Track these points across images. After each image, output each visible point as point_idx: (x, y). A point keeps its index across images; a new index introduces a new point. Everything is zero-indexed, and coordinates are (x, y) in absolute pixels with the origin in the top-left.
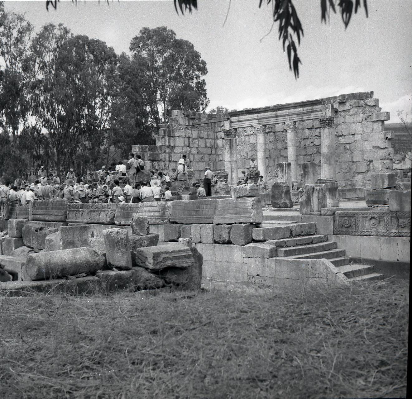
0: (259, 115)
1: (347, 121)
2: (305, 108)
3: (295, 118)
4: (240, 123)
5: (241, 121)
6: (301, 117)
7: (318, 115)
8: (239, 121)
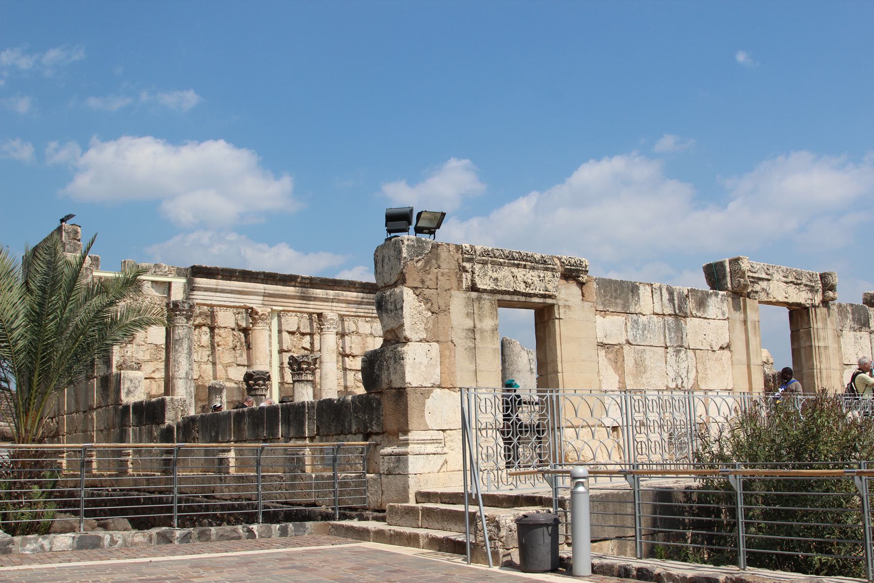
6: (354, 310)
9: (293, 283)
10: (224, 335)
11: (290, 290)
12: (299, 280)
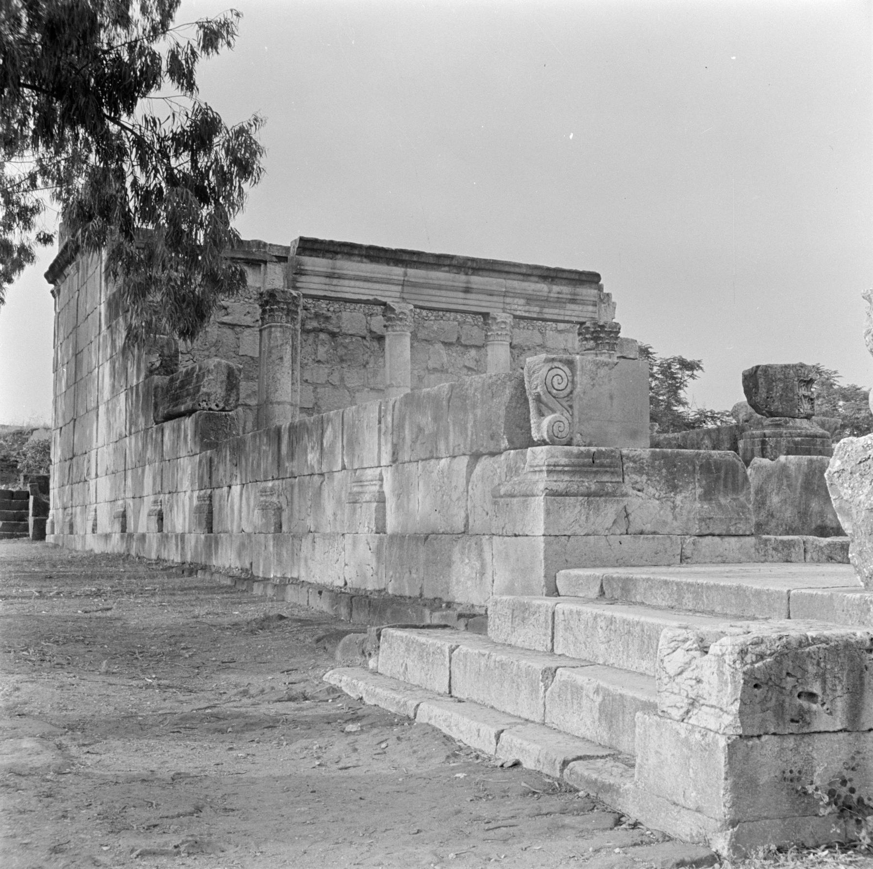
0: (411, 271)
1: (549, 344)
2: (556, 288)
3: (520, 307)
4: (335, 281)
5: (340, 277)
6: (537, 309)
7: (585, 314)
8: (330, 276)
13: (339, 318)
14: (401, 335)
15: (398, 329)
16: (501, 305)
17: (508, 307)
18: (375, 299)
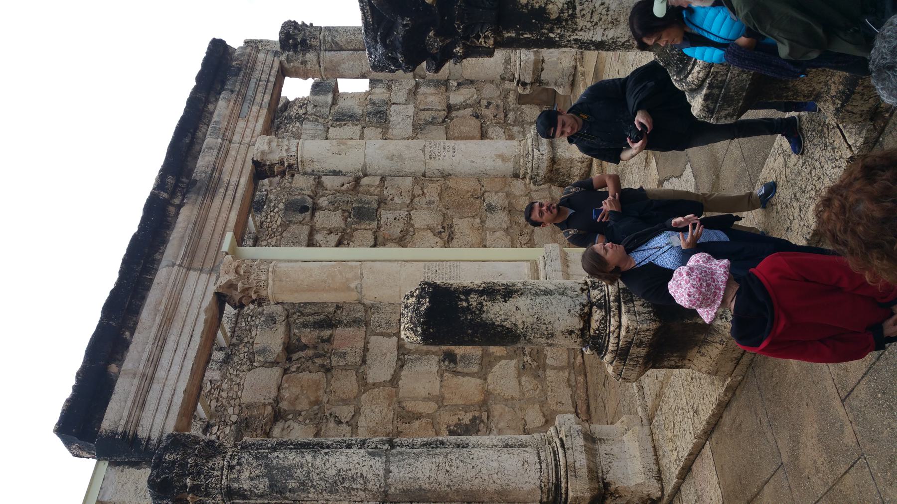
6: (255, 109)
9: (172, 210)
10: (296, 390)
11: (185, 217)
12: (164, 195)
13: (249, 407)
14: (274, 272)
15: (263, 278)
16: (243, 148)
17: (247, 140)
18: (206, 311)
